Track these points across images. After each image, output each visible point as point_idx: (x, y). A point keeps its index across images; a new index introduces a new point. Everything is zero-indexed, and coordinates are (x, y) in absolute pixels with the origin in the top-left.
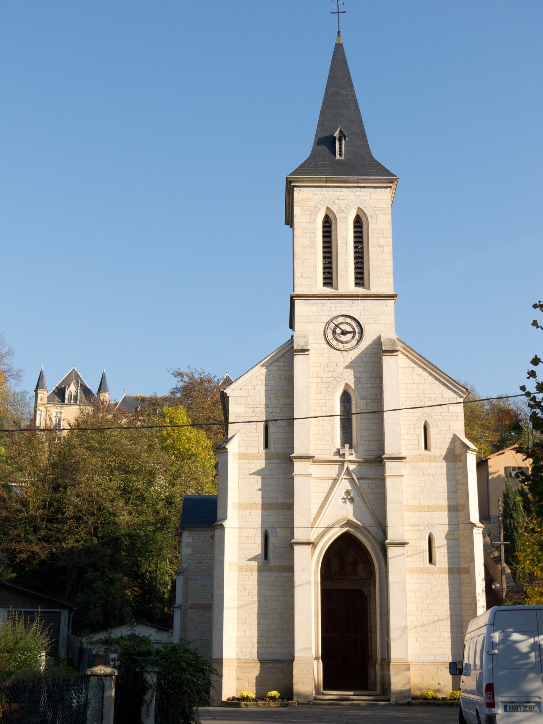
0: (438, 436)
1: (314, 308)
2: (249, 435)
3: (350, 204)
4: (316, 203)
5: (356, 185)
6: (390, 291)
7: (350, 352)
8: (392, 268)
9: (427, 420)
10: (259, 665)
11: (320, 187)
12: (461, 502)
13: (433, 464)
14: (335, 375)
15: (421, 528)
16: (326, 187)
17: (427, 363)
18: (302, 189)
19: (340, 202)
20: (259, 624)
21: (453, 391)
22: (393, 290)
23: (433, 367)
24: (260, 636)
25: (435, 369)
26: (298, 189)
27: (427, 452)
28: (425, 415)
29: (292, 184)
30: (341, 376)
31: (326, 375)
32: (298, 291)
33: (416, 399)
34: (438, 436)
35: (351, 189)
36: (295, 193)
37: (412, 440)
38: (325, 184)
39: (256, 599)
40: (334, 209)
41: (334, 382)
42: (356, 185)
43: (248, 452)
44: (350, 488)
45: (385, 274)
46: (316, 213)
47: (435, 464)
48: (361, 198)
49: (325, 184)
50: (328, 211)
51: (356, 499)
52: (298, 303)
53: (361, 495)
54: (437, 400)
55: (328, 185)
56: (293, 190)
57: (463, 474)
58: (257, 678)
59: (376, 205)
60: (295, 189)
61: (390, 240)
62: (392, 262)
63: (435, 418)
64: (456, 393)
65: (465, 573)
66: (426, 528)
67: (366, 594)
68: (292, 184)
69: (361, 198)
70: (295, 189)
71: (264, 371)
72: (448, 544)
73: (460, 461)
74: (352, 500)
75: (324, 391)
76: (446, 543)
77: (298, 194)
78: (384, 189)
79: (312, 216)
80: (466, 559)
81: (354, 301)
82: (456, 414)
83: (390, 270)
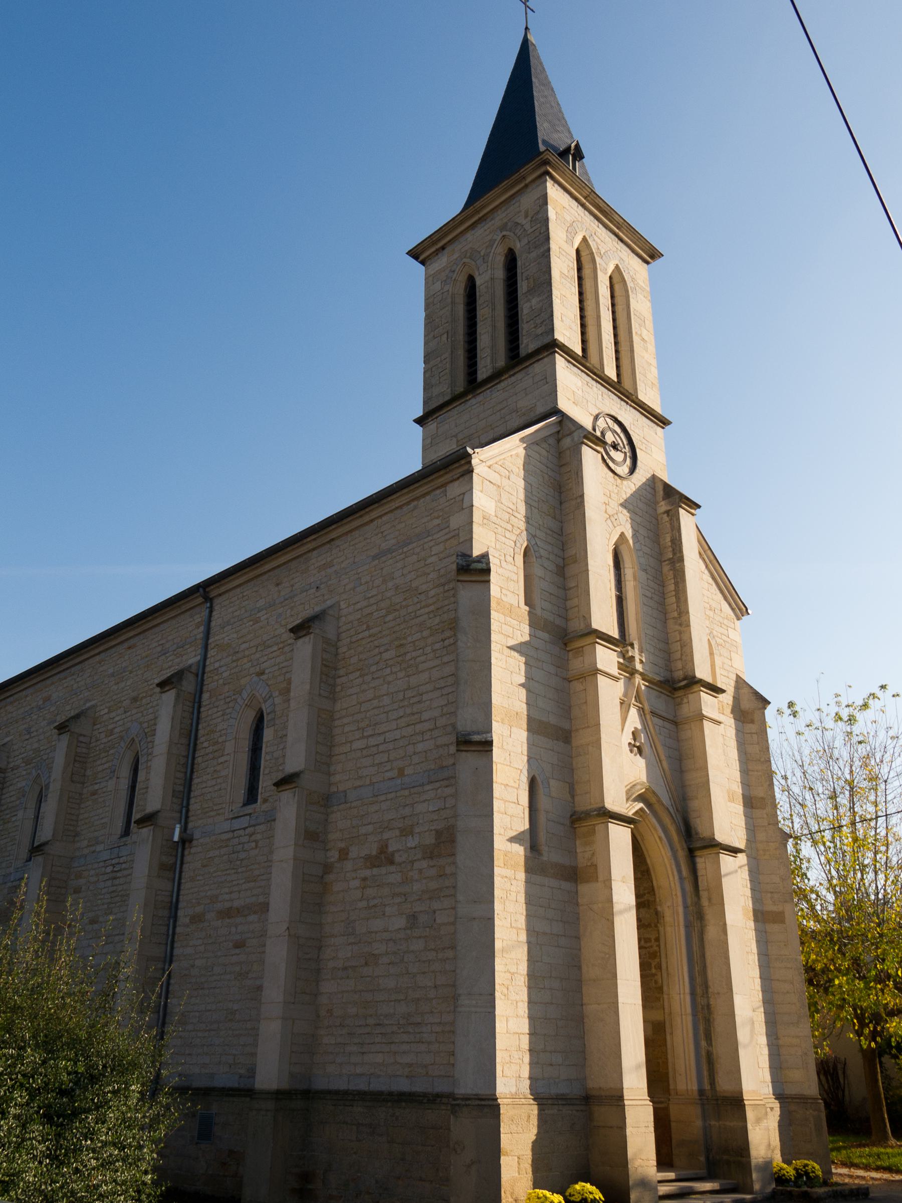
2: (504, 564)
10: (535, 1110)
11: (576, 199)
12: (759, 792)
16: (583, 205)
17: (707, 548)
20: (530, 1002)
21: (730, 605)
23: (712, 557)
24: (533, 1034)
25: (715, 562)
39: (523, 937)
44: (639, 727)
50: (583, 244)
51: (647, 749)
53: (653, 746)
57: (758, 743)
58: (534, 1143)
64: (733, 609)
65: (774, 922)
71: (521, 451)
72: (748, 864)
73: (752, 722)
74: (640, 751)
76: (746, 862)
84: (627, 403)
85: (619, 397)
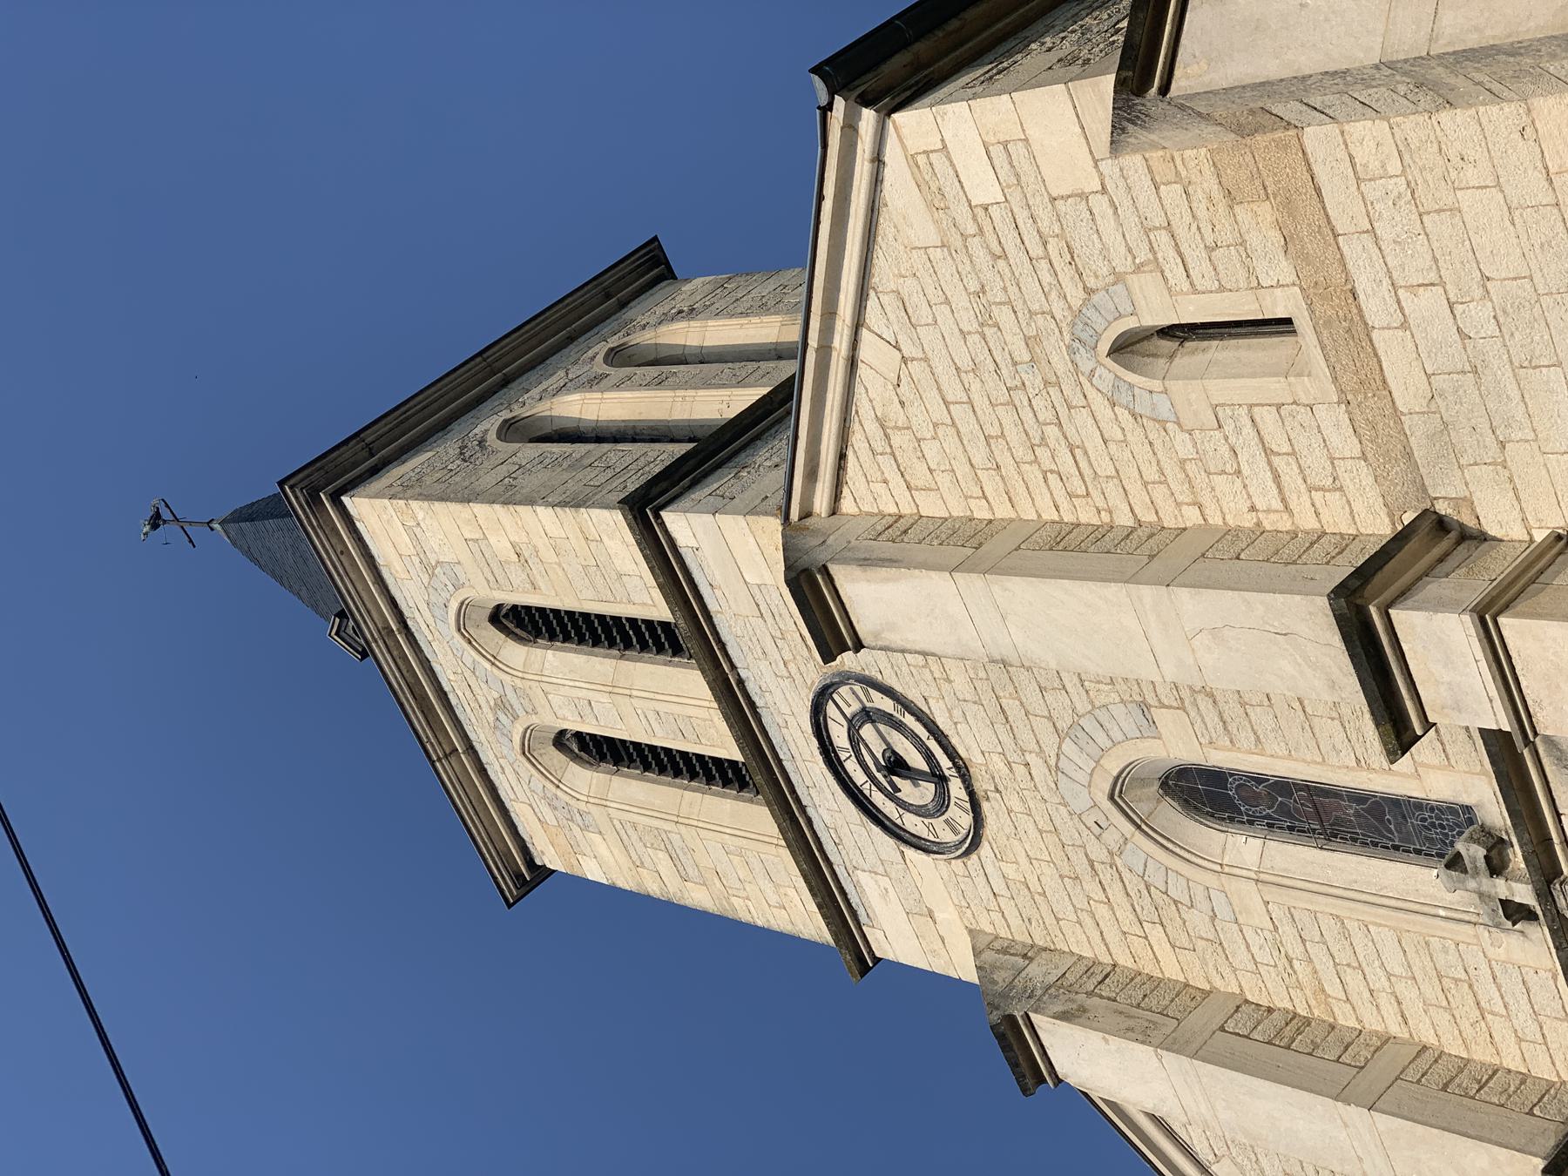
9: (1104, 346)
54: (973, 286)
63: (1076, 296)
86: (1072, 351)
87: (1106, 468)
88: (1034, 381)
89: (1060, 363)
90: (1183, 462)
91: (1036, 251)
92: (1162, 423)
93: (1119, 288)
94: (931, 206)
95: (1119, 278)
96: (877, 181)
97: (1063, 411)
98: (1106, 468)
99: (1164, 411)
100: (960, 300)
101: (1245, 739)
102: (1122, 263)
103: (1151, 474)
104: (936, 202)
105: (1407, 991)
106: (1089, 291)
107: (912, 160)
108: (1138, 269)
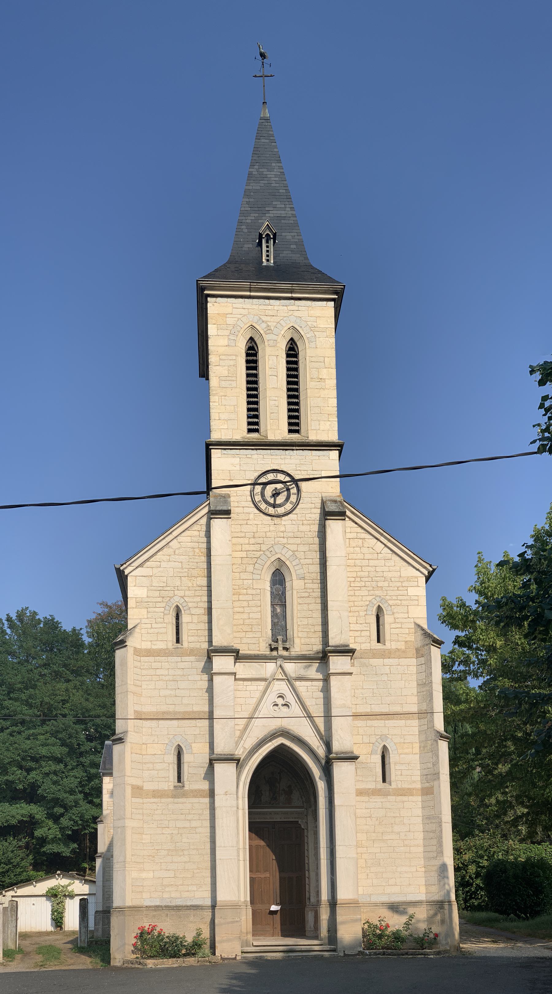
0: (393, 626)
1: (237, 460)
3: (282, 322)
4: (236, 319)
5: (289, 295)
6: (333, 437)
7: (283, 518)
8: (336, 409)
9: (381, 605)
13: (387, 661)
14: (264, 548)
15: (373, 740)
18: (219, 300)
19: (268, 318)
22: (337, 438)
26: (214, 299)
27: (379, 646)
28: (378, 599)
29: (205, 292)
30: (272, 549)
31: (252, 548)
32: (215, 436)
33: (367, 579)
34: (393, 626)
35: (283, 301)
36: (209, 305)
37: (361, 631)
38: (248, 293)
40: (261, 328)
41: (263, 557)
42: (289, 295)
43: (154, 647)
45: (327, 416)
46: (236, 333)
47: (391, 660)
48: (297, 314)
49: (248, 293)
52: (215, 454)
54: (393, 579)
55: (253, 294)
56: (207, 302)
59: (315, 324)
60: (209, 299)
61: (334, 371)
62: (335, 401)
63: (391, 602)
66: (379, 740)
67: (303, 827)
68: (205, 292)
69: (297, 314)
70: (209, 299)
75: (250, 568)
77: (214, 307)
78: (325, 302)
79: (232, 337)
80: (429, 777)
81: (287, 452)
82: (416, 598)
83: (334, 411)
84: (293, 450)
85: (283, 450)
86: (380, 597)
87: (357, 593)
88: (374, 584)
89: (378, 593)
90: (359, 612)
91: (399, 598)
92: (366, 611)
93: (391, 613)
94: (408, 577)
95: (393, 613)
96: (414, 567)
97: (368, 589)
98: (357, 593)
99: (369, 613)
100: (390, 575)
101: (300, 601)
102: (396, 615)
103: (356, 603)
104: (408, 579)
105: (245, 616)
106: (391, 606)
107: (417, 577)
108: (395, 619)
